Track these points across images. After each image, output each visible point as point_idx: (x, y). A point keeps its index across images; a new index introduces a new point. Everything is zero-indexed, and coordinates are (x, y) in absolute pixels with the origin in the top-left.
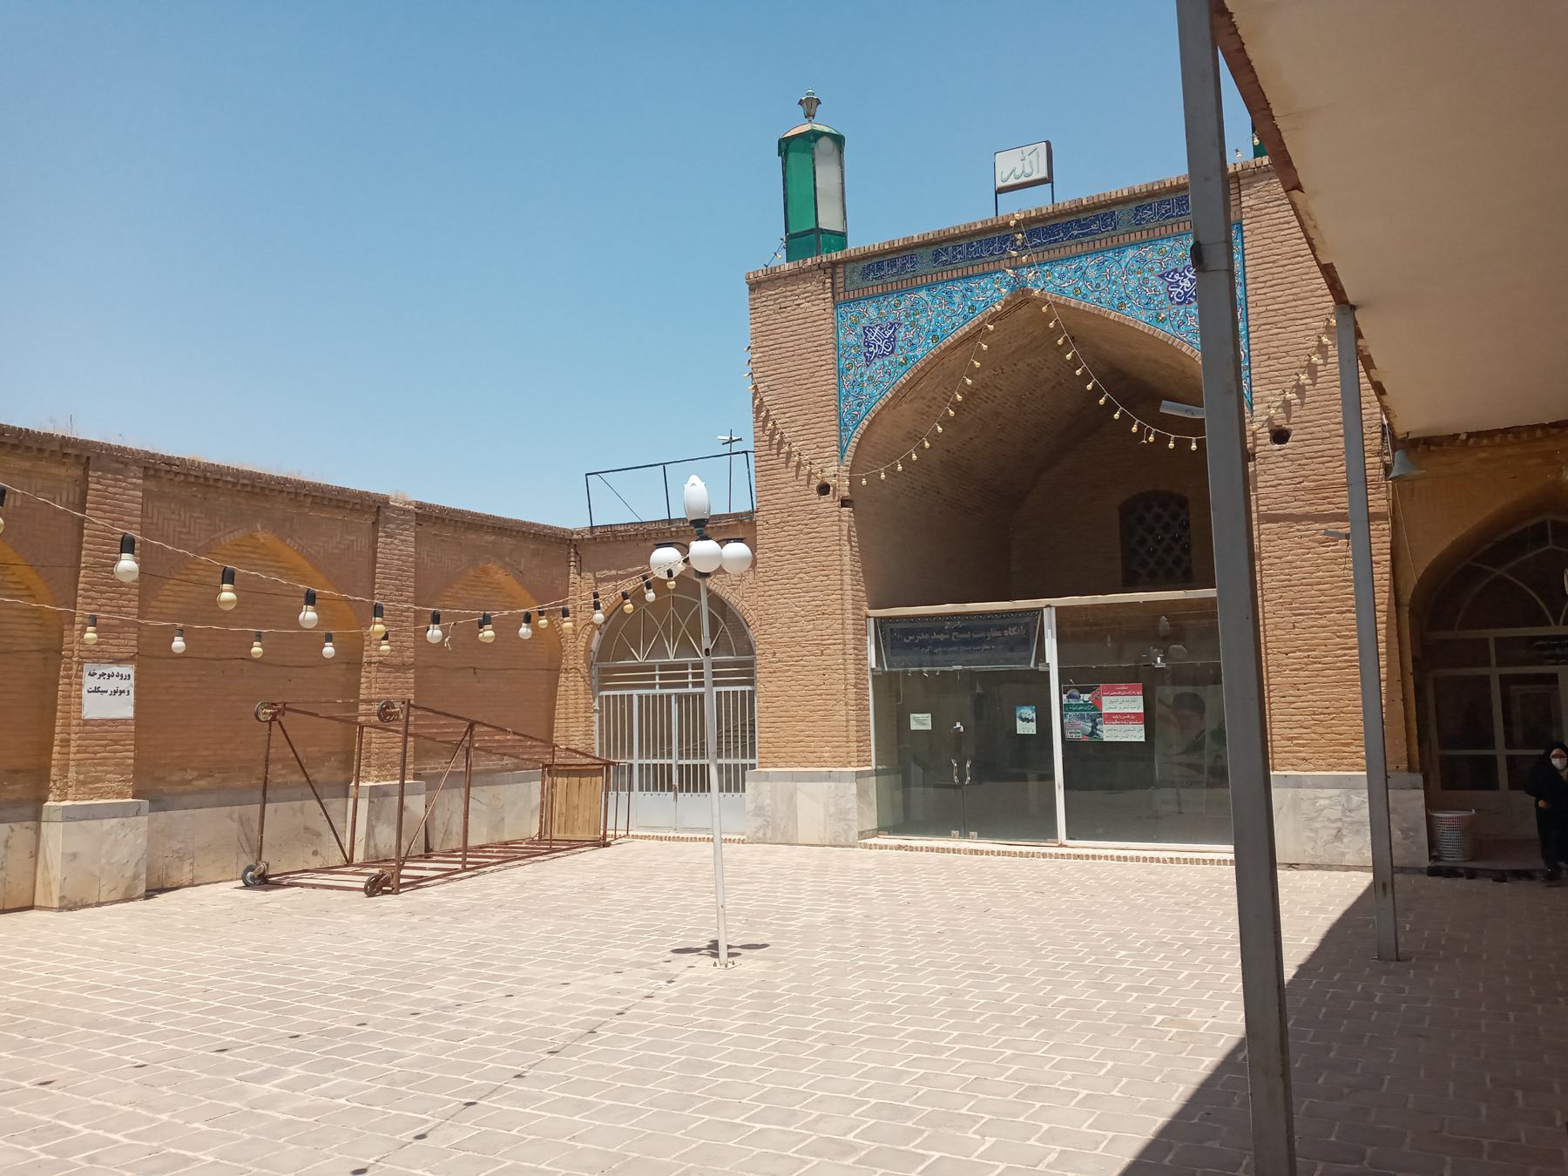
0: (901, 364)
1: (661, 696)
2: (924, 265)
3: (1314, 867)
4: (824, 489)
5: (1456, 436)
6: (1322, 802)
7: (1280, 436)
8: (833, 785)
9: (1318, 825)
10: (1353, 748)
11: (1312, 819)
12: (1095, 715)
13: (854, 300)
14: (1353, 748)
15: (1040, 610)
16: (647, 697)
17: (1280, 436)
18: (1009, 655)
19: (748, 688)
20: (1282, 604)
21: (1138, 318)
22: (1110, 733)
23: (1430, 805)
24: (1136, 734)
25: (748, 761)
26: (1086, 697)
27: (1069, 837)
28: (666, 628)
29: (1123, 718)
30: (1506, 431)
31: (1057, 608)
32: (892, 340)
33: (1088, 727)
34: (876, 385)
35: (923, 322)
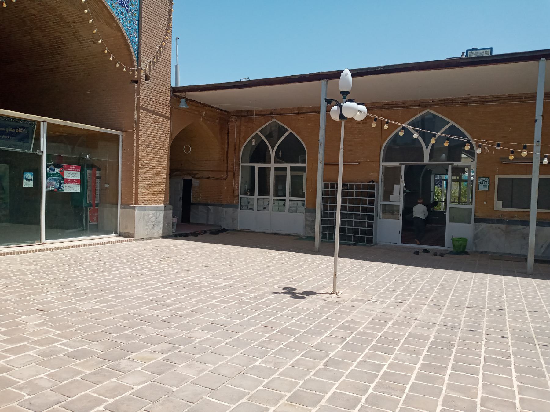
3: (147, 239)
6: (151, 216)
9: (149, 224)
10: (157, 197)
11: (147, 222)
12: (62, 180)
14: (157, 197)
15: (39, 122)
17: (147, 78)
18: (18, 143)
20: (144, 142)
22: (68, 188)
24: (76, 189)
26: (57, 170)
27: (46, 239)
29: (72, 181)
31: (49, 124)
33: (57, 185)
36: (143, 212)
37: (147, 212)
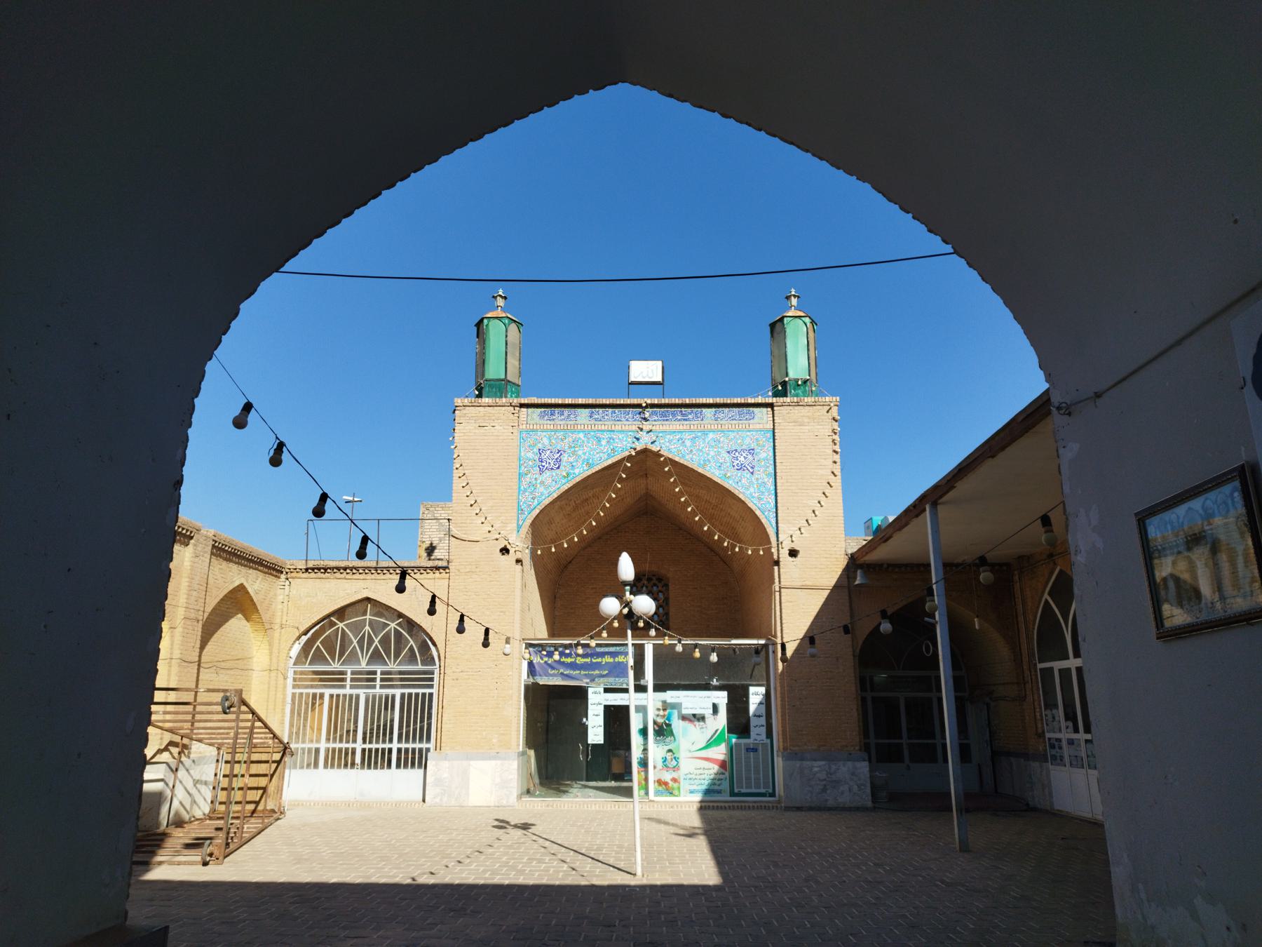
1: (351, 696)
4: (505, 551)
5: (881, 565)
7: (793, 553)
8: (499, 762)
13: (533, 430)
16: (338, 696)
19: (427, 691)
21: (714, 473)
23: (871, 771)
25: (424, 745)
28: (361, 642)
30: (906, 565)
32: (559, 461)
34: (546, 488)
35: (580, 453)
36: (798, 764)
37: (807, 763)
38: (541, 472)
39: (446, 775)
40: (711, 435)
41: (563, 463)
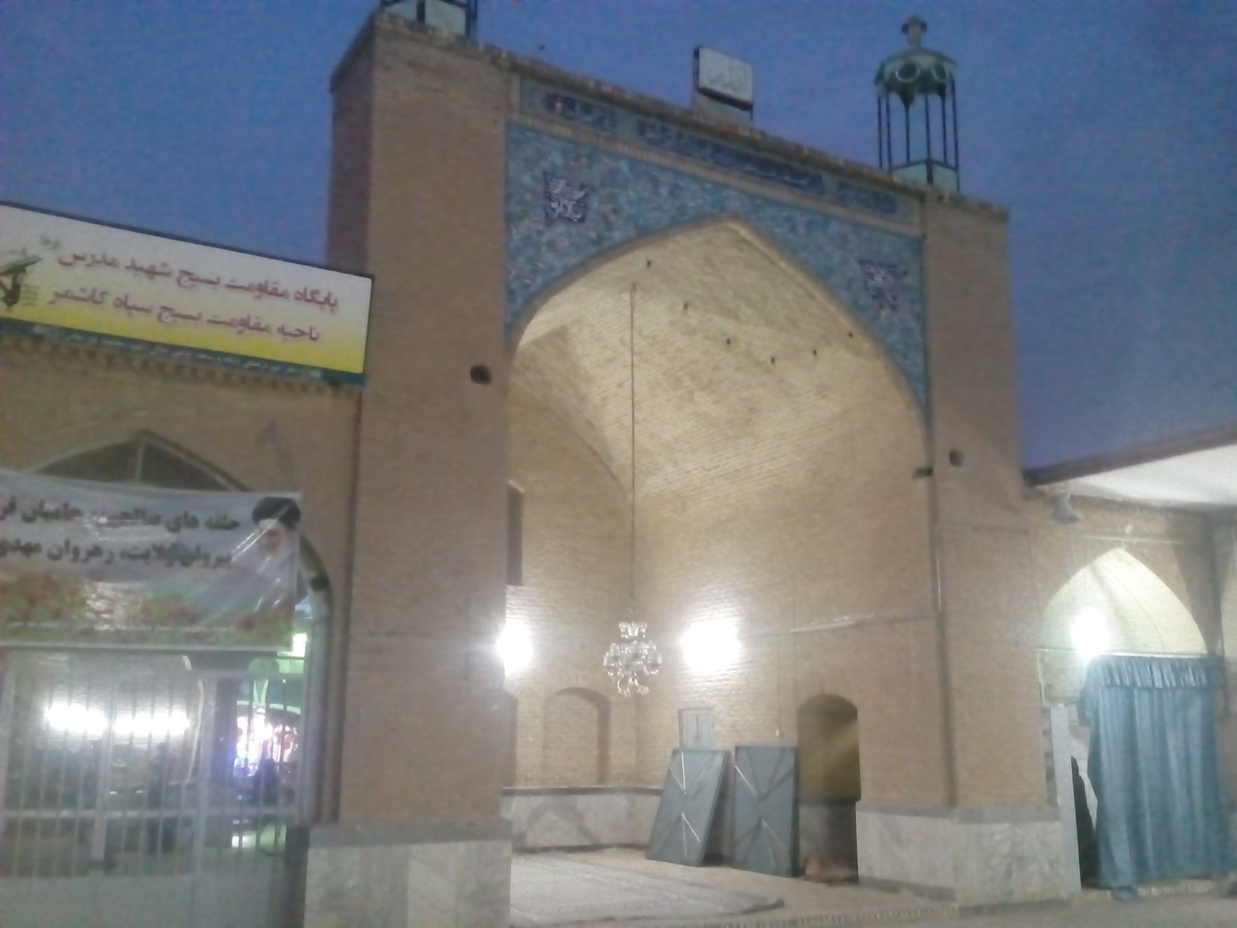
0: (593, 242)
2: (627, 125)
8: (473, 845)
32: (581, 205)
35: (622, 200)
38: (549, 220)
39: (351, 883)
40: (834, 227)
41: (591, 215)
